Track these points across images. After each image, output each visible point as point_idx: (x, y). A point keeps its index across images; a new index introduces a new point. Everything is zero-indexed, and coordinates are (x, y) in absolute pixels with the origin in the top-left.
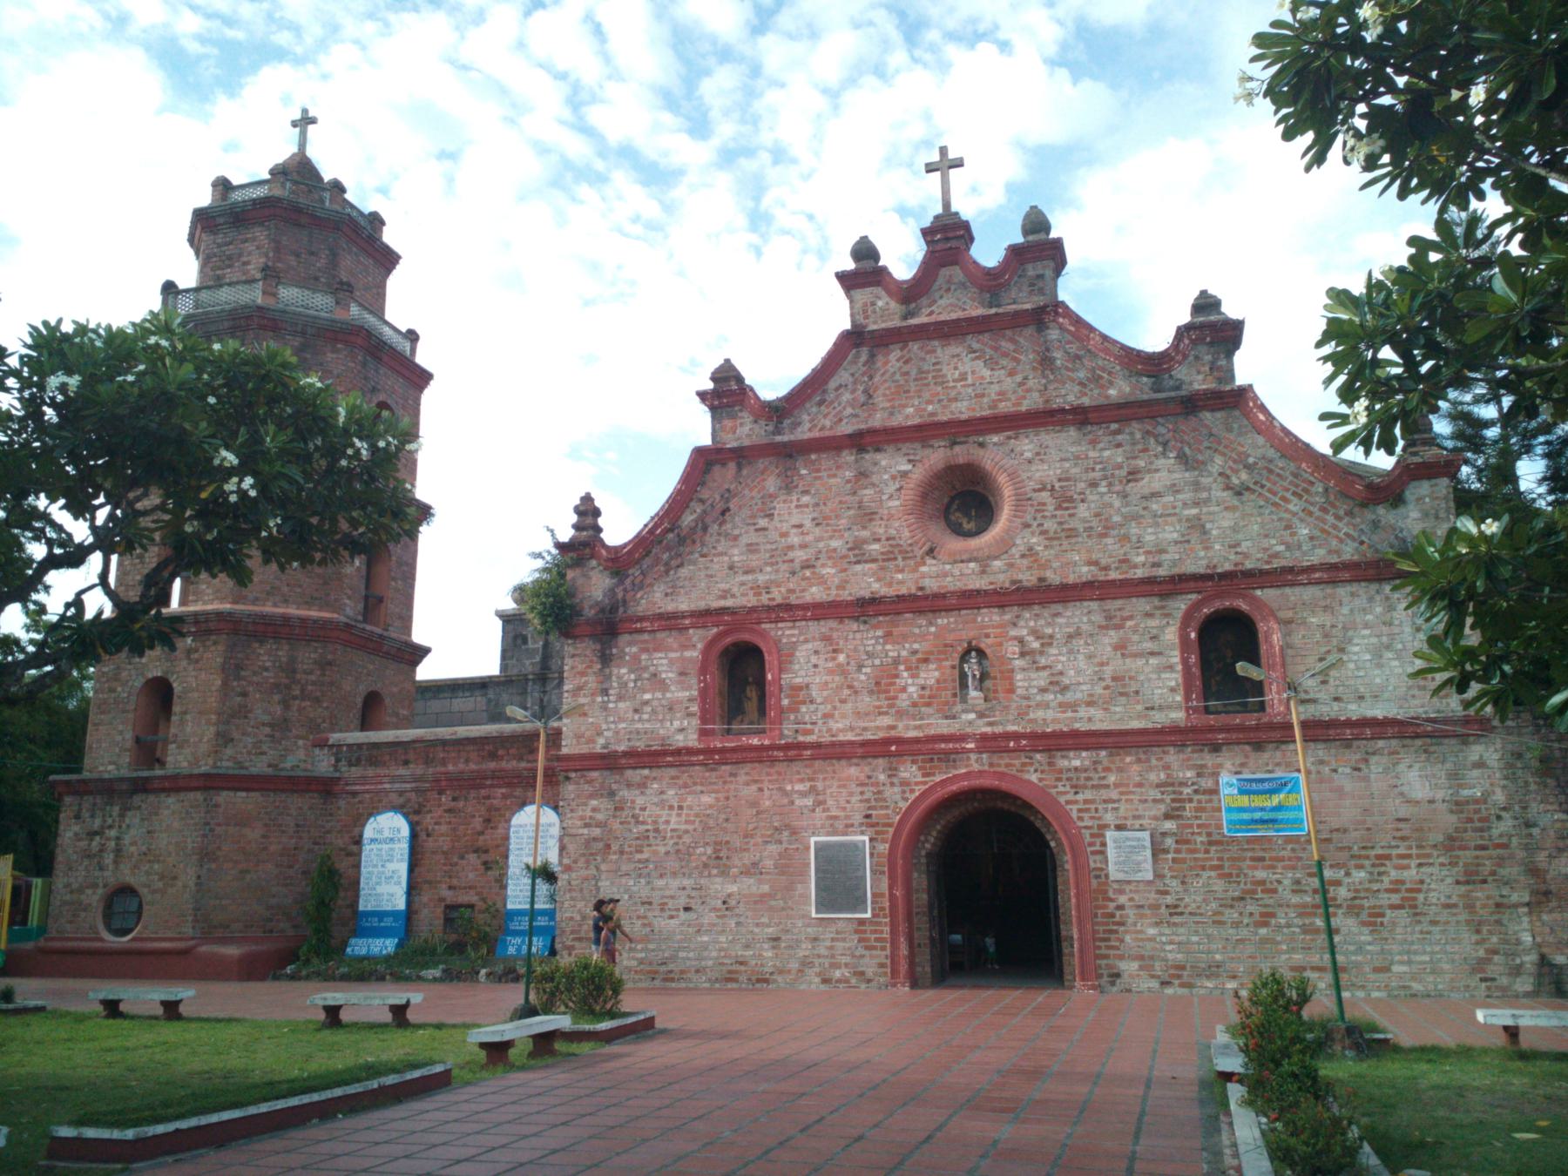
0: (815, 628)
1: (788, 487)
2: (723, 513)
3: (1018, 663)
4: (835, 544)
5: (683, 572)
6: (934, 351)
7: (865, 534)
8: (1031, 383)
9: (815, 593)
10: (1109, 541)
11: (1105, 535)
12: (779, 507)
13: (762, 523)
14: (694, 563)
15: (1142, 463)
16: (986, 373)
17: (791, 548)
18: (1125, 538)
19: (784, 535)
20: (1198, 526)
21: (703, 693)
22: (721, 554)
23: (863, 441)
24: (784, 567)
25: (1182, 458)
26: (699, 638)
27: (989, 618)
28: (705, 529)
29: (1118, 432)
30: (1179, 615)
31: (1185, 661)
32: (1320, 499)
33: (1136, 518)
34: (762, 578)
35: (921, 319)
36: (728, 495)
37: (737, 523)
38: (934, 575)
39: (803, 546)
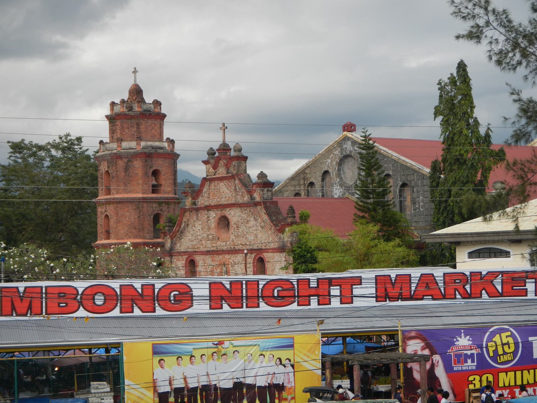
0: (202, 257)
1: (197, 219)
2: (188, 225)
3: (231, 268)
4: (205, 235)
5: (182, 240)
6: (219, 184)
7: (209, 233)
8: (233, 194)
9: (202, 249)
10: (244, 238)
11: (243, 237)
12: (197, 225)
13: (194, 228)
14: (183, 238)
15: (249, 219)
16: (227, 191)
17: (198, 235)
18: (246, 238)
19: (197, 232)
20: (256, 236)
21: (186, 272)
22: (188, 236)
23: (208, 208)
24: (197, 240)
25: (254, 218)
26: (185, 257)
27: (227, 256)
28: (185, 229)
29: (245, 210)
30: (253, 258)
31: (254, 270)
32: (273, 231)
33: (247, 233)
34: (194, 243)
35: (217, 176)
36: (188, 220)
37: (190, 229)
38: (221, 245)
39: (200, 235)
